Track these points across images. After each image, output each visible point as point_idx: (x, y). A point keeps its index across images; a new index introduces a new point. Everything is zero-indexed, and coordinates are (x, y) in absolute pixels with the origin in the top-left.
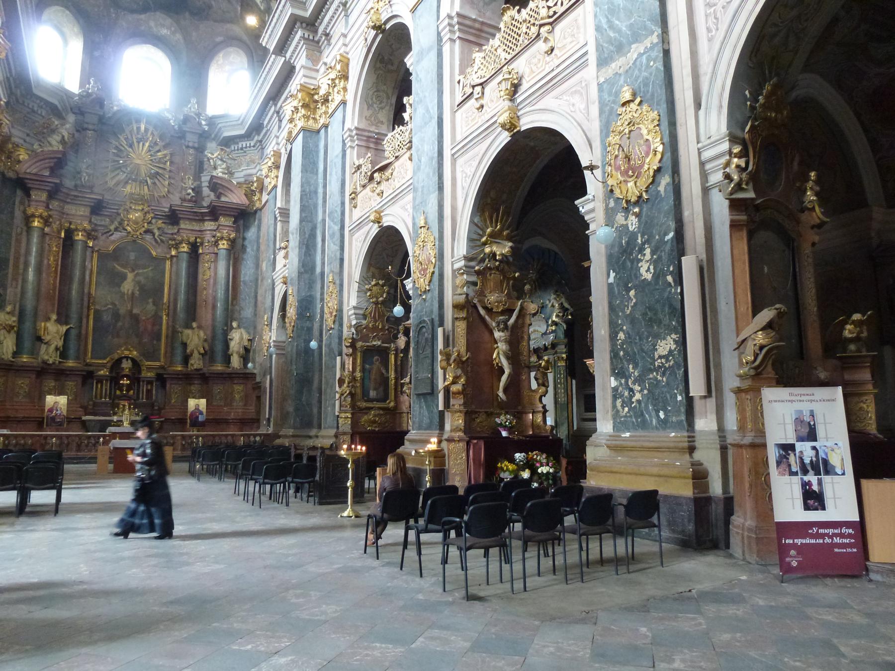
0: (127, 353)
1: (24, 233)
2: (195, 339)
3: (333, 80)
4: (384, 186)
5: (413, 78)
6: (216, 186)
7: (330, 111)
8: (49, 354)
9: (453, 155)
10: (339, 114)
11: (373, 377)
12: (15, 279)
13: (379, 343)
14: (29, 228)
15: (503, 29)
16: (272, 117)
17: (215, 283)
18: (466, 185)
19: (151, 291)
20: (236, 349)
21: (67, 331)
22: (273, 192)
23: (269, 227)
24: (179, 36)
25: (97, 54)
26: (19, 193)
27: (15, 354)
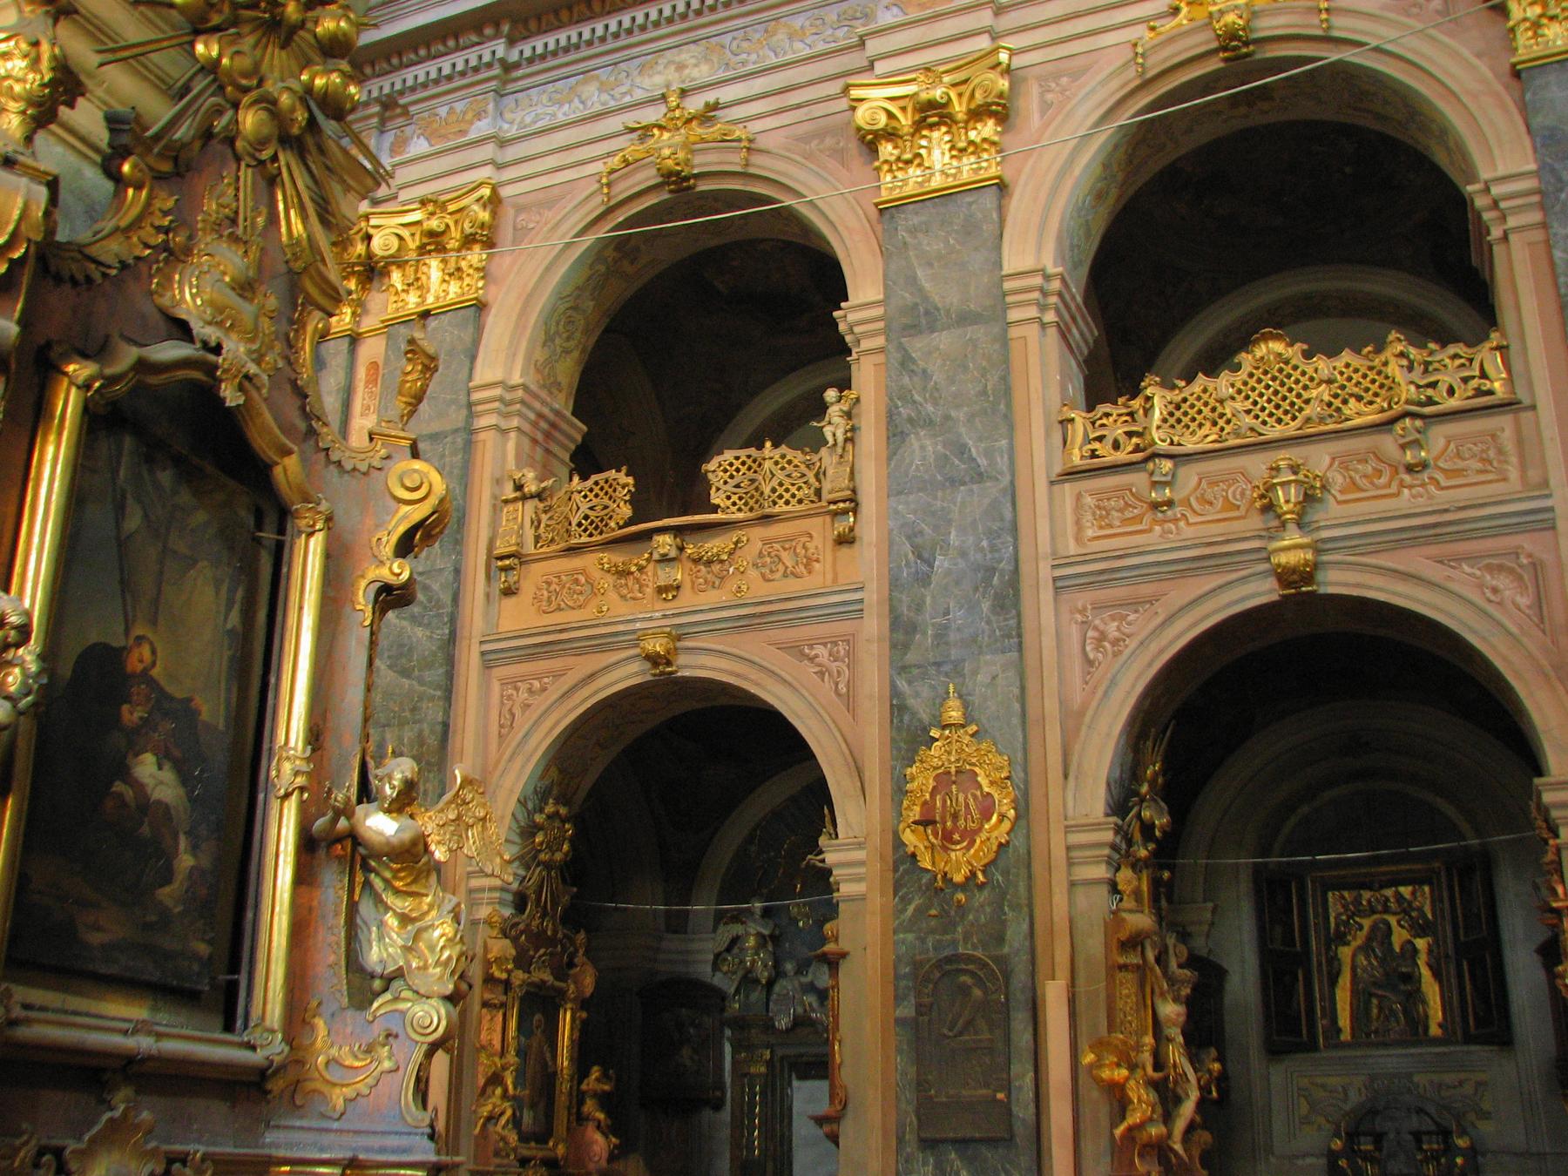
15: (1247, 368)
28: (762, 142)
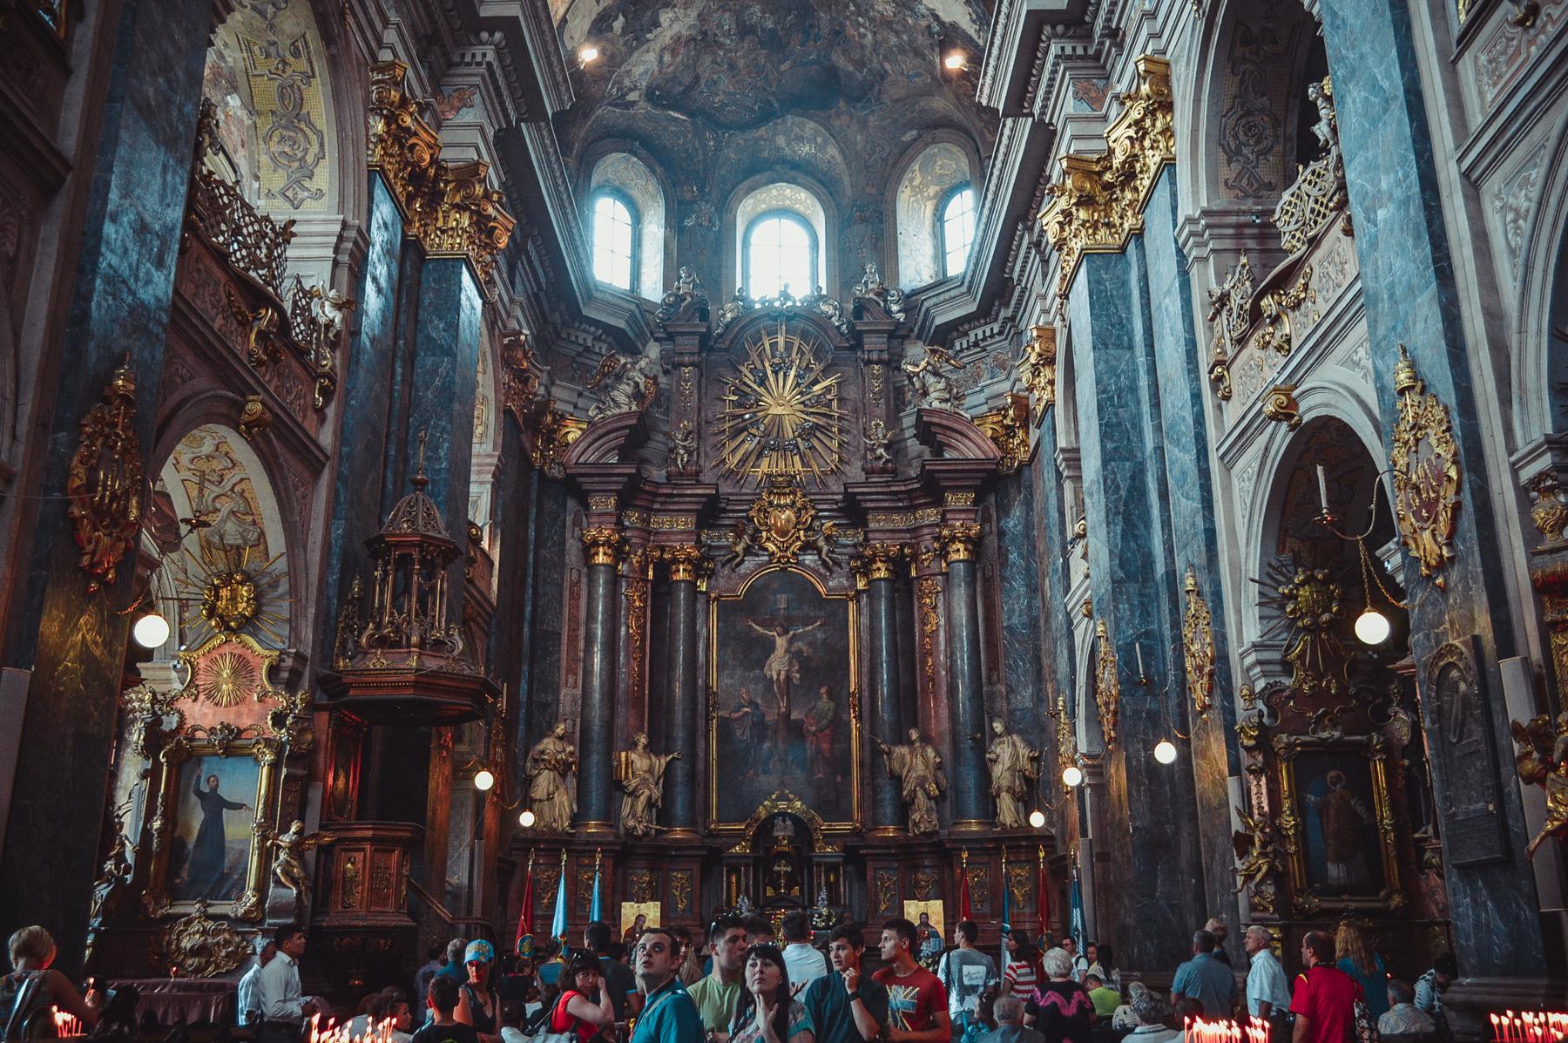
0: (782, 805)
1: (584, 580)
2: (916, 763)
3: (1137, 122)
5: (1326, 31)
6: (927, 431)
7: (1142, 195)
8: (634, 815)
9: (1466, 175)
10: (1162, 193)
12: (572, 671)
13: (1337, 734)
14: (592, 568)
16: (1026, 258)
18: (1520, 242)
19: (823, 668)
20: (1005, 783)
21: (668, 764)
22: (1048, 418)
24: (832, 151)
25: (689, 223)
26: (571, 504)
27: (576, 820)
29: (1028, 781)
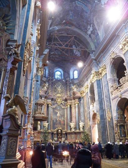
0: (59, 128)
2: (72, 125)
4: (120, 90)
11: (122, 132)
17: (76, 113)
23: (87, 100)
28: (117, 53)
29: (83, 127)
